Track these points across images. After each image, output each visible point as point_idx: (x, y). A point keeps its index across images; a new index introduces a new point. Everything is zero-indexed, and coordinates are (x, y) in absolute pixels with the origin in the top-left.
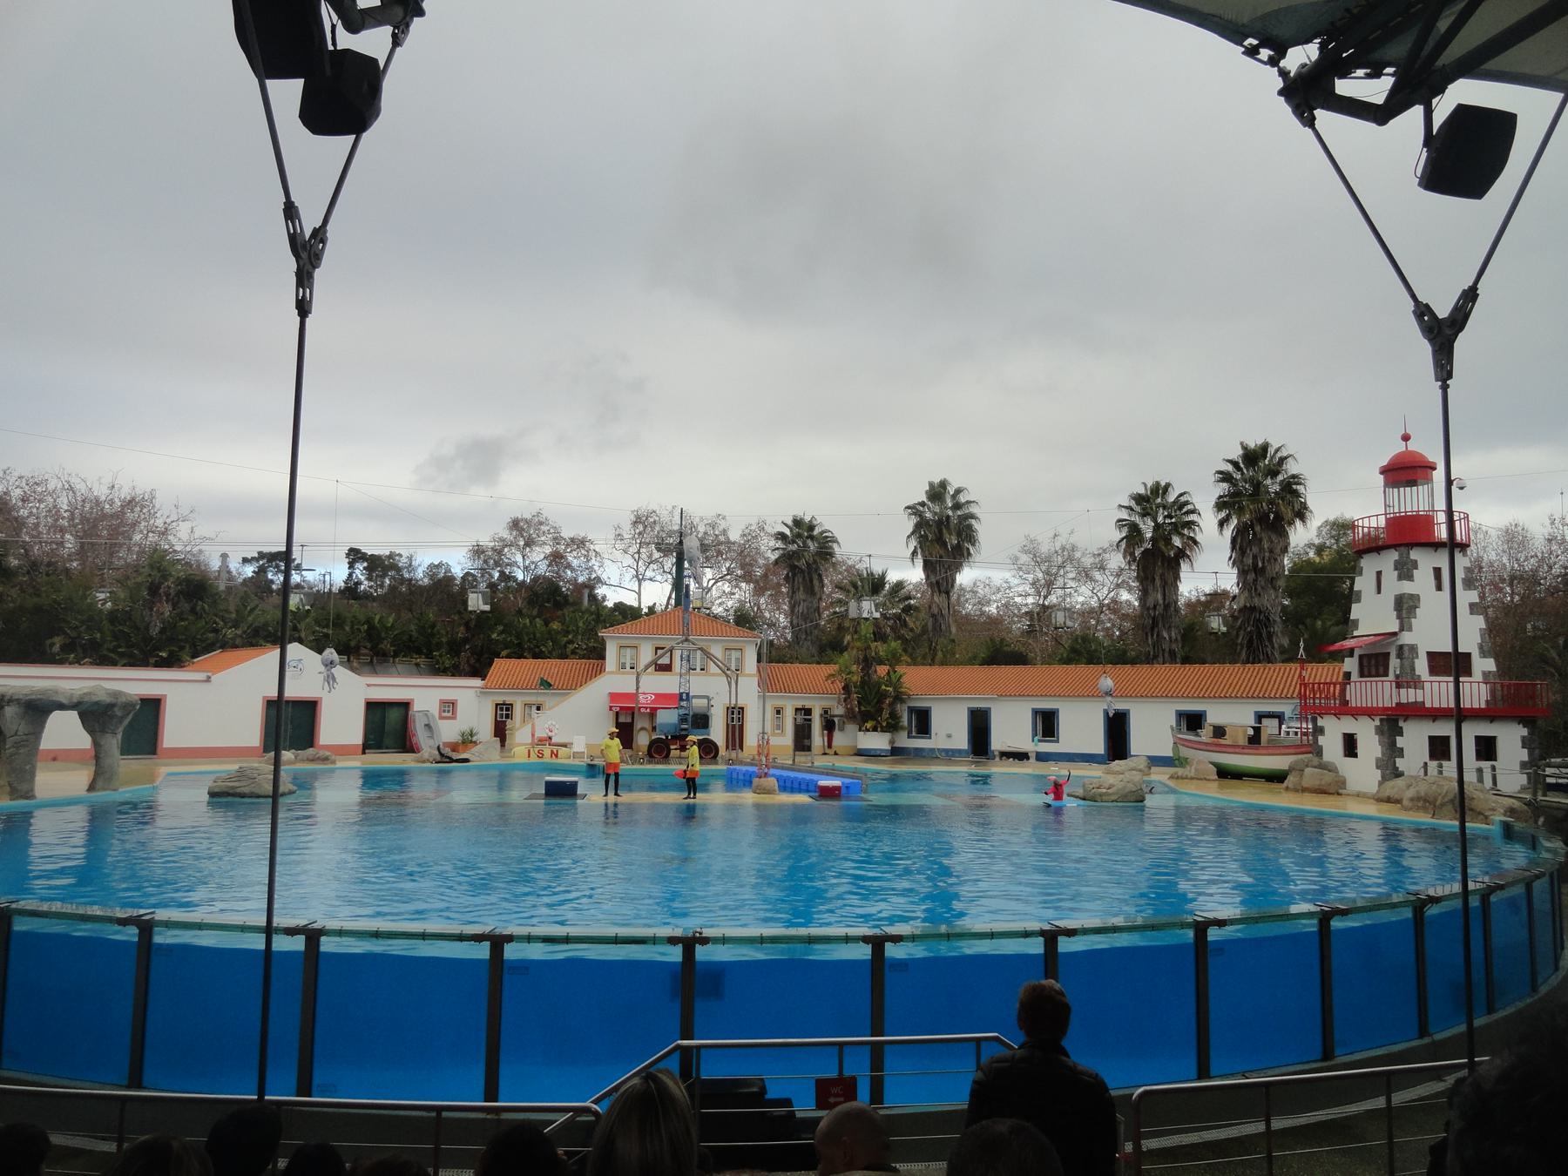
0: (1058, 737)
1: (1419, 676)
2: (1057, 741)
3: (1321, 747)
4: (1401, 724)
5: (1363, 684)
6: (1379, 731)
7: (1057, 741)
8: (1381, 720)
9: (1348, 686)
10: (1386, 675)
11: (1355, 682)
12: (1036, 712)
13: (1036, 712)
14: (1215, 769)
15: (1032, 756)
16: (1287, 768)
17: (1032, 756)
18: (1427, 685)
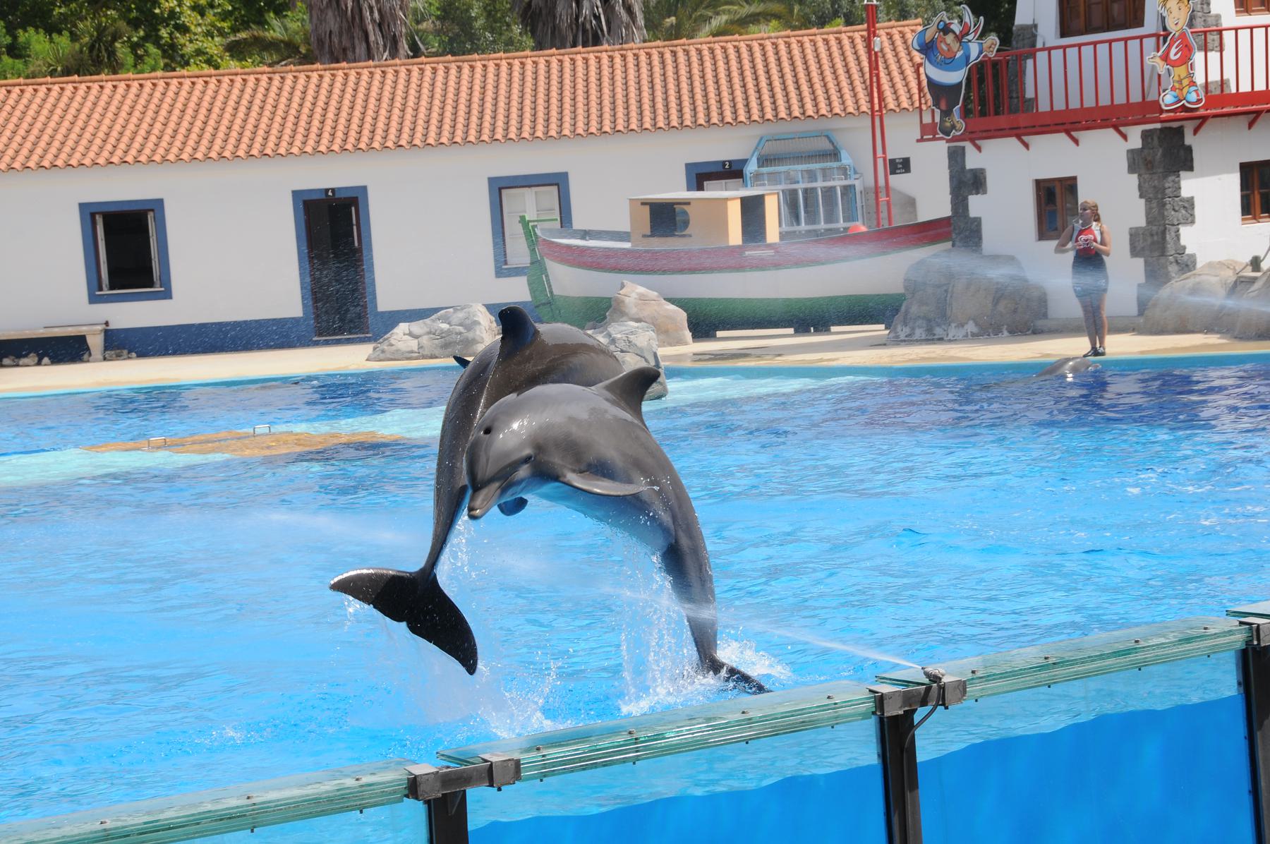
0: (166, 283)
1: (1218, 17)
2: (167, 295)
3: (978, 221)
4: (1189, 139)
5: (1072, 53)
6: (1137, 162)
7: (167, 295)
8: (1146, 135)
9: (1030, 63)
10: (1139, 22)
11: (1050, 49)
12: (90, 213)
13: (90, 213)
14: (682, 316)
15: (96, 342)
16: (901, 290)
17: (96, 342)
18: (1228, 37)
